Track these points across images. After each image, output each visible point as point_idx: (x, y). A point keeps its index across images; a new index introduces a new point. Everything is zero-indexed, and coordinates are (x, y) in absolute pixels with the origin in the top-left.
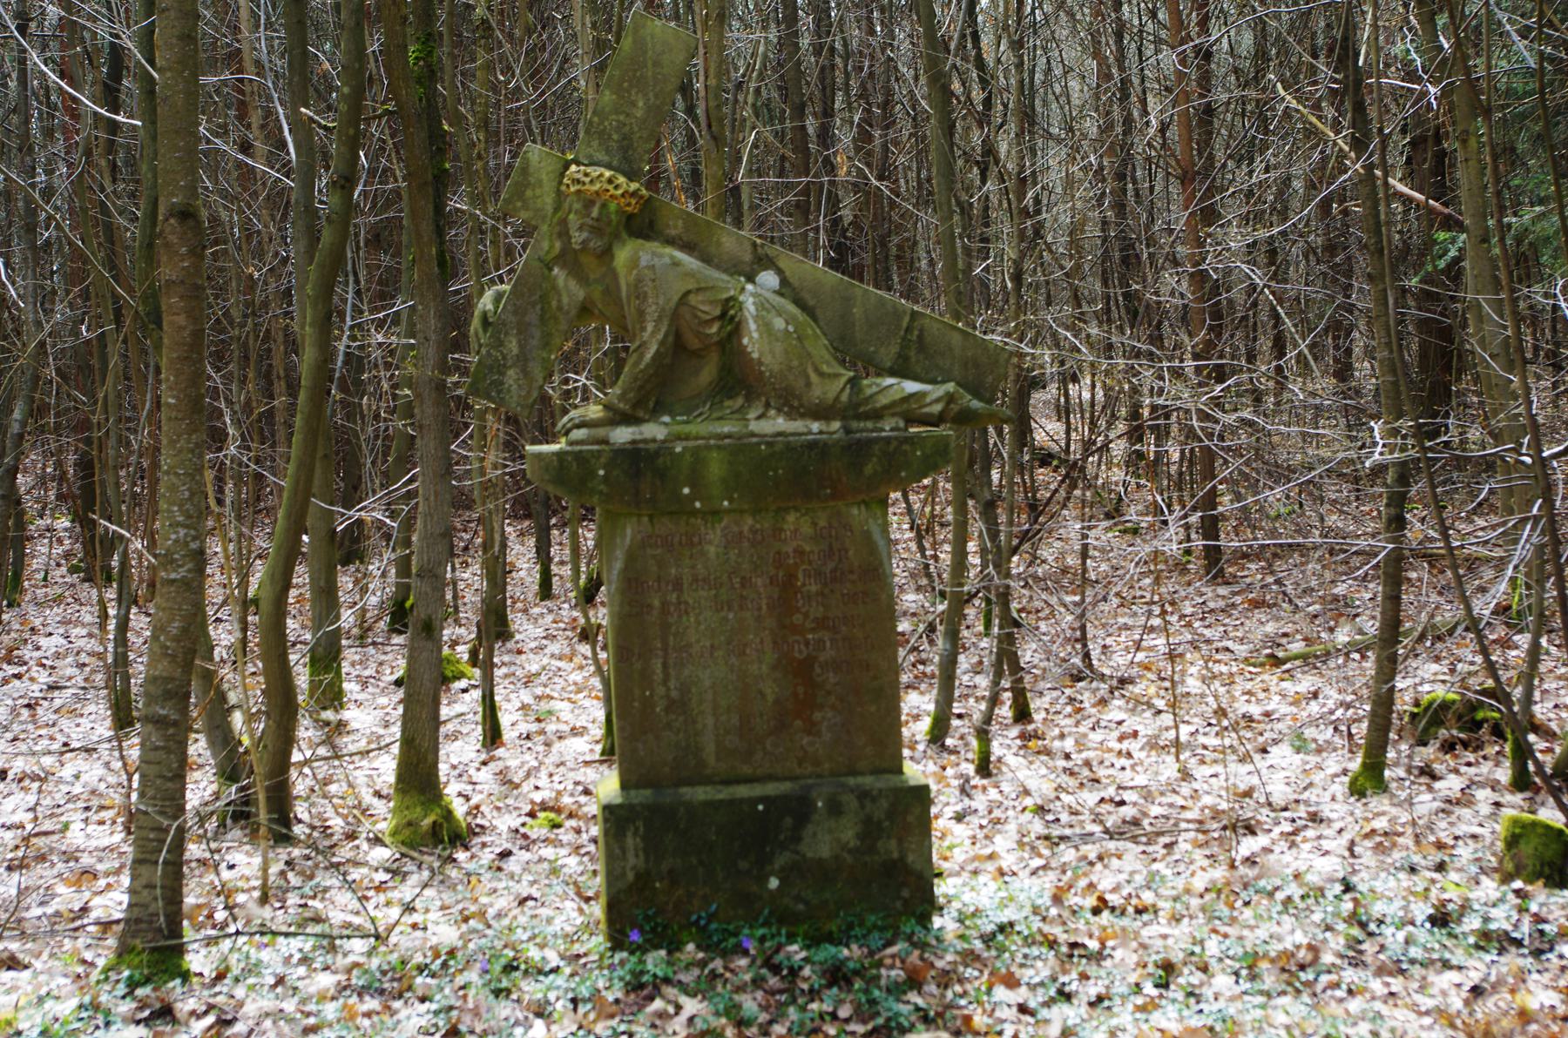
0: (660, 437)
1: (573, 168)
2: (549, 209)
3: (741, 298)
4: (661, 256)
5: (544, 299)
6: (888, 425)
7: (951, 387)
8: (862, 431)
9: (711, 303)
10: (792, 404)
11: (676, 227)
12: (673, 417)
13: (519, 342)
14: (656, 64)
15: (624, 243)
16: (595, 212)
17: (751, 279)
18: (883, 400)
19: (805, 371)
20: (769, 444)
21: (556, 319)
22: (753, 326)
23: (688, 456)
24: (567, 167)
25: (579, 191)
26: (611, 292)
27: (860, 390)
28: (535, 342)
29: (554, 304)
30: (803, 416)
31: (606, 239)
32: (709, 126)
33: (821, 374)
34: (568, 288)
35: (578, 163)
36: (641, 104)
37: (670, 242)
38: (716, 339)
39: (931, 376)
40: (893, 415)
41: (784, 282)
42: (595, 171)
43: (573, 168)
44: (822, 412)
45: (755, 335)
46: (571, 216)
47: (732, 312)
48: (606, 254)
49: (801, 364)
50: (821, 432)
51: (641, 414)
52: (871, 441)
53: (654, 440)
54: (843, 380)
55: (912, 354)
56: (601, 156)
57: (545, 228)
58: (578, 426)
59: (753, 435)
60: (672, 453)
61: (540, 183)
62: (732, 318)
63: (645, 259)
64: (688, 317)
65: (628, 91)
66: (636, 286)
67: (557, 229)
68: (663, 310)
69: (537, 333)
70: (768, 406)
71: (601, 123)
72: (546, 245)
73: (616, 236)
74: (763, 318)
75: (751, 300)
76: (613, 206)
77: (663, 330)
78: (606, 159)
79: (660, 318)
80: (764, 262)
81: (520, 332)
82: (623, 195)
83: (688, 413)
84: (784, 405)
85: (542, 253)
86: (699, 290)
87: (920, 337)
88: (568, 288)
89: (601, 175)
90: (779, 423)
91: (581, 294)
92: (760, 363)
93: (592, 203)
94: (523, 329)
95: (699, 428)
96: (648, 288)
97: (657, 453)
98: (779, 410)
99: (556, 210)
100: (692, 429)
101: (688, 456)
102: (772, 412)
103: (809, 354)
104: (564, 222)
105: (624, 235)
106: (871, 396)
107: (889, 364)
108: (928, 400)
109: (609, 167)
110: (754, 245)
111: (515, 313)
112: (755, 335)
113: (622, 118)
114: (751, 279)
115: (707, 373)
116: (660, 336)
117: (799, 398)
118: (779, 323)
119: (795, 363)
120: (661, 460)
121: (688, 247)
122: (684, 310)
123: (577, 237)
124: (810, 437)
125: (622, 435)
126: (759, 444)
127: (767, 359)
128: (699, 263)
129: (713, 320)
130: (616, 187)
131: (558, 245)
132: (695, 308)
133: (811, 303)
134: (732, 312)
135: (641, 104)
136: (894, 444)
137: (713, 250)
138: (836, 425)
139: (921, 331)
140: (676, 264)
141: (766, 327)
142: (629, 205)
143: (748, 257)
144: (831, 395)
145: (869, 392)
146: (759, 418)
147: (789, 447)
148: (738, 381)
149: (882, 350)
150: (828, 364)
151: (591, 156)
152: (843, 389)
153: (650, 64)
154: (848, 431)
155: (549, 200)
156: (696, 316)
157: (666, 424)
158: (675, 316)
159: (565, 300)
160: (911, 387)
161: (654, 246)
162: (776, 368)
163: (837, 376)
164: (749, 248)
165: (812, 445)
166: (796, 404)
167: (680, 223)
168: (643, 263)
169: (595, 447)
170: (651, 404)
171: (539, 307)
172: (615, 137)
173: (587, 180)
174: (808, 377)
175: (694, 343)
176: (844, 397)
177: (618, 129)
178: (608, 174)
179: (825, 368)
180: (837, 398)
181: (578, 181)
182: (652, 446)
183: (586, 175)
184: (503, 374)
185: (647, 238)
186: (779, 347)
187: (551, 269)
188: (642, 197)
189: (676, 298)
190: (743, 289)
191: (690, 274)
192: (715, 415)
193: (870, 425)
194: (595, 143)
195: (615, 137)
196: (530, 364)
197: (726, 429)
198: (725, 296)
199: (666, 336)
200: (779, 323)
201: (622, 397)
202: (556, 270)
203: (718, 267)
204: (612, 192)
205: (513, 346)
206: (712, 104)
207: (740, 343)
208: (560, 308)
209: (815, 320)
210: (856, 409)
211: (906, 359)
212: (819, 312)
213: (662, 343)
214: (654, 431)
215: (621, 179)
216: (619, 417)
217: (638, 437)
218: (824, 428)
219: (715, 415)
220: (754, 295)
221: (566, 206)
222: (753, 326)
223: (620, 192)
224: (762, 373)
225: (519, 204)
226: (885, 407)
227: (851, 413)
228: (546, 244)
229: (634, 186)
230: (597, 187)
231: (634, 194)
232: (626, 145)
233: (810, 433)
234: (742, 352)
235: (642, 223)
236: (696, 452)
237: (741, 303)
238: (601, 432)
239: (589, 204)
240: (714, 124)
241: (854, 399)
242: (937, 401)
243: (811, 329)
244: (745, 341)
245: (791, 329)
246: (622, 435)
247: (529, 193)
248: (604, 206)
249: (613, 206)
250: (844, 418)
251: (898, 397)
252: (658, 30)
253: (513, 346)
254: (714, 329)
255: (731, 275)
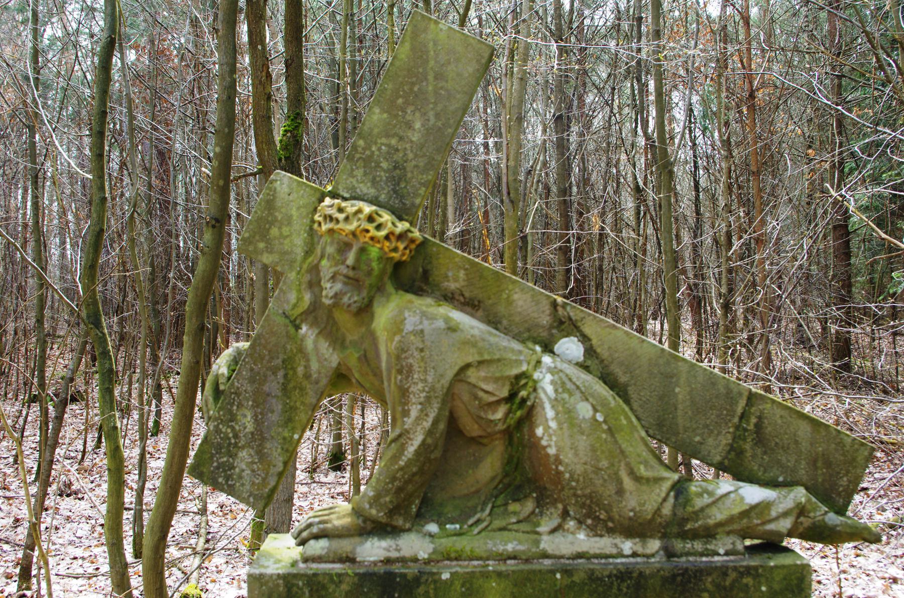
0: (423, 555)
1: (328, 201)
2: (299, 252)
3: (536, 375)
4: (432, 318)
5: (288, 364)
6: (722, 545)
7: (800, 494)
8: (688, 554)
9: (496, 380)
10: (597, 515)
11: (456, 280)
12: (441, 525)
13: (255, 416)
14: (439, 76)
15: (388, 297)
16: (351, 259)
17: (548, 348)
18: (718, 515)
19: (616, 474)
20: (567, 572)
21: (302, 389)
22: (550, 413)
23: (457, 585)
24: (321, 200)
25: (331, 231)
26: (368, 359)
27: (688, 501)
28: (274, 417)
29: (300, 370)
30: (611, 531)
31: (365, 293)
32: (509, 193)
33: (638, 479)
34: (318, 351)
35: (334, 195)
36: (418, 125)
37: (449, 298)
38: (501, 427)
39: (770, 475)
40: (728, 533)
41: (590, 351)
42: (351, 207)
43: (328, 201)
44: (635, 529)
45: (553, 424)
46: (324, 262)
47: (523, 393)
48: (365, 311)
49: (613, 465)
50: (635, 555)
51: (399, 522)
52: (700, 573)
53: (415, 560)
54: (667, 485)
55: (747, 446)
56: (366, 189)
57: (292, 275)
58: (317, 537)
59: (545, 555)
60: (434, 578)
61: (289, 220)
62: (524, 401)
63: (411, 322)
64: (466, 397)
65: (404, 111)
66: (398, 358)
67: (307, 278)
68: (433, 389)
69: (278, 407)
70: (565, 514)
71: (368, 147)
72: (293, 297)
73: (379, 289)
74: (564, 402)
75: (549, 377)
76: (374, 252)
77: (430, 420)
78: (372, 192)
79: (428, 399)
80: (566, 326)
81: (256, 405)
82: (387, 237)
83: (461, 519)
84: (588, 516)
85: (287, 307)
86: (480, 363)
87: (759, 426)
88: (318, 351)
89: (360, 211)
90: (580, 540)
91: (333, 359)
92: (558, 461)
93: (347, 246)
94: (260, 401)
95: (476, 542)
96: (414, 360)
97: (417, 580)
98: (580, 522)
99: (308, 253)
100: (464, 544)
101: (457, 585)
102: (571, 524)
103: (622, 452)
104: (315, 269)
105: (390, 288)
106: (702, 509)
107: (718, 458)
108: (774, 514)
109: (371, 202)
110: (554, 304)
111: (252, 380)
112: (553, 424)
113: (393, 142)
114: (548, 348)
115: (490, 466)
116: (427, 424)
117: (608, 509)
118: (584, 410)
119: (604, 463)
120: (421, 590)
121: (470, 305)
122: (463, 391)
123: (330, 289)
124: (619, 560)
125: (373, 550)
126: (553, 572)
127: (568, 457)
128: (483, 327)
129: (498, 402)
130: (379, 227)
131: (307, 297)
132: (475, 386)
133: (623, 379)
134: (523, 393)
135: (418, 125)
136: (733, 575)
137: (502, 309)
138: (654, 545)
139: (760, 418)
140: (452, 329)
141: (567, 415)
142: (395, 250)
143: (545, 319)
144: (650, 507)
145: (699, 503)
146: (553, 531)
147: (592, 577)
148: (527, 479)
149: (710, 441)
150: (646, 463)
151: (353, 188)
152: (665, 500)
153: (431, 78)
154: (670, 554)
155: (298, 242)
156: (476, 397)
157: (431, 535)
158: (449, 395)
159: (314, 366)
160: (753, 494)
161: (425, 303)
162: (579, 469)
163: (658, 480)
164: (547, 309)
165: (624, 575)
166: (603, 516)
167: (462, 274)
168: (408, 327)
169: (337, 567)
170: (414, 509)
171: (281, 374)
172: (384, 165)
173: (341, 216)
174: (620, 482)
175: (472, 429)
176: (667, 510)
177: (388, 156)
178: (368, 209)
179: (642, 471)
180: (658, 510)
181: (331, 218)
182: (411, 571)
183: (341, 210)
184: (233, 456)
185: (418, 291)
186: (583, 442)
187: (298, 328)
188: (413, 241)
189: (450, 374)
190: (539, 362)
191: (471, 343)
192: (498, 523)
193: (698, 546)
194: (359, 173)
195: (384, 165)
196: (268, 445)
197: (510, 547)
198: (515, 371)
199: (435, 422)
200: (584, 410)
201: (375, 501)
202: (304, 328)
203: (506, 331)
204: (373, 232)
205: (247, 421)
206: (511, 178)
207: (532, 433)
208: (307, 376)
209: (627, 401)
210: (682, 524)
211: (740, 453)
212: (631, 390)
213: (430, 433)
214: (415, 545)
215: (386, 217)
216: (370, 527)
217: (394, 555)
218: (640, 550)
219: (498, 523)
220: (552, 371)
221: (318, 251)
222: (550, 413)
223: (383, 233)
224: (559, 473)
225: (261, 245)
226: (720, 524)
227: (675, 530)
228: (293, 296)
229: (402, 226)
230: (353, 226)
231: (401, 237)
232: (397, 176)
233: (621, 555)
234: (534, 444)
235: (412, 273)
236: (469, 580)
237: (535, 382)
238: (345, 546)
239: (344, 247)
240: (512, 192)
241: (680, 512)
242: (785, 514)
243: (626, 419)
244: (539, 431)
245: (600, 417)
246: (373, 550)
247: (274, 231)
248: (363, 250)
249: (374, 252)
250: (664, 536)
251: (736, 511)
252: (442, 36)
253: (247, 421)
254: (499, 414)
255: (523, 342)
